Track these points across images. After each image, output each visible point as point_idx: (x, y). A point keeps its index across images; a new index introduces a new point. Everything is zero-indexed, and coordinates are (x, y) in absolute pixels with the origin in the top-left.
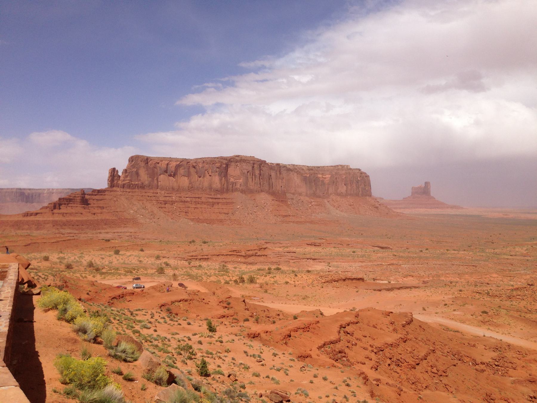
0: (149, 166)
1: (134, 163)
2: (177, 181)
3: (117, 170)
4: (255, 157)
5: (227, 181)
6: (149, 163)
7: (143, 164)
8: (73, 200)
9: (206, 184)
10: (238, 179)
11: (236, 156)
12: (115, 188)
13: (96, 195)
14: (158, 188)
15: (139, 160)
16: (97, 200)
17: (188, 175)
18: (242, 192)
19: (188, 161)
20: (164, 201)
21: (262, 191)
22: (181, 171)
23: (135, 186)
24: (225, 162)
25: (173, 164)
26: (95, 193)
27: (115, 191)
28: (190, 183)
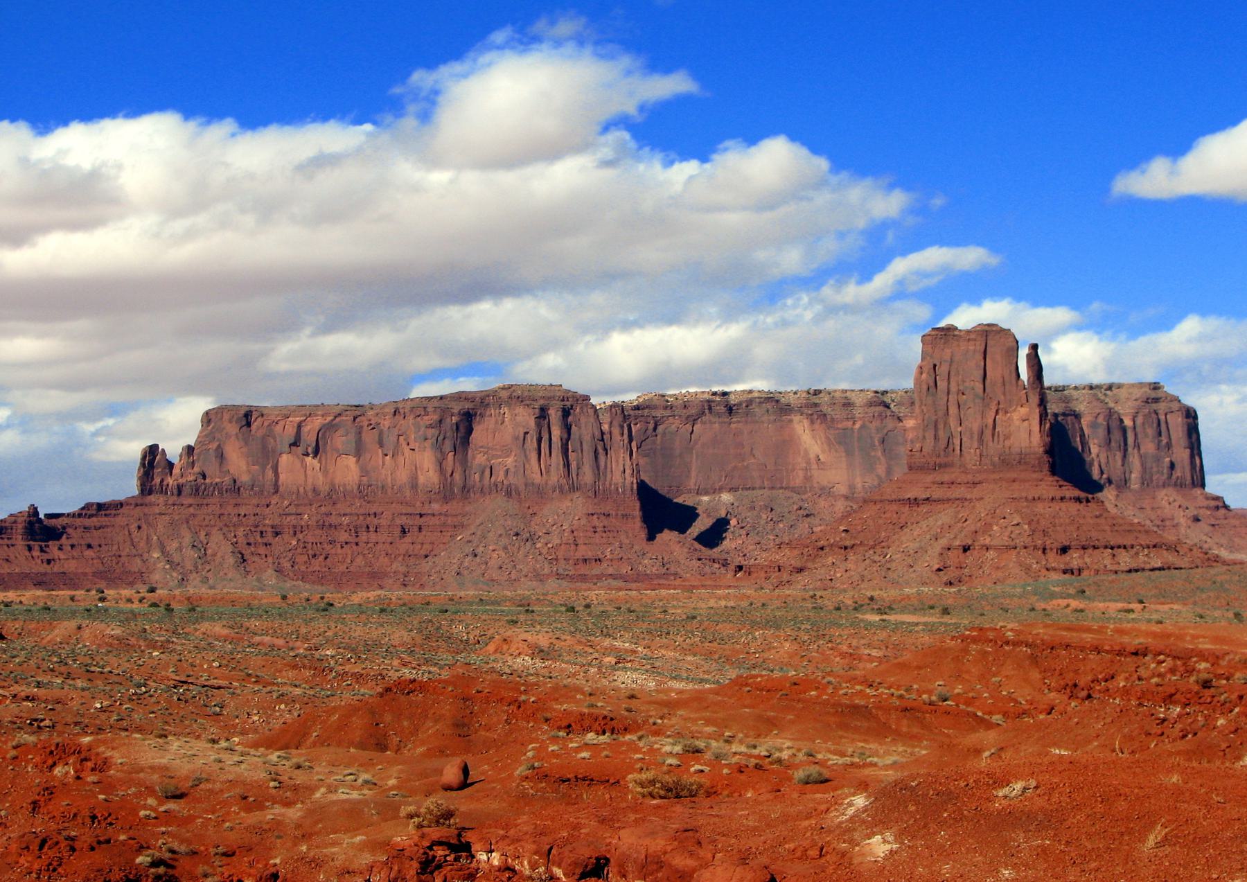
0: (253, 432)
1: (213, 428)
2: (325, 472)
3: (163, 450)
4: (564, 387)
5: (464, 463)
6: (254, 426)
7: (232, 429)
8: (9, 531)
9: (403, 476)
10: (500, 457)
11: (503, 388)
12: (152, 498)
13: (91, 516)
14: (276, 492)
15: (226, 417)
16: (85, 528)
17: (359, 452)
18: (509, 494)
19: (357, 412)
20: (272, 527)
21: (573, 488)
22: (341, 440)
23: (211, 489)
24: (457, 408)
25: (317, 422)
26: (89, 512)
27: (151, 504)
28: (364, 471)
